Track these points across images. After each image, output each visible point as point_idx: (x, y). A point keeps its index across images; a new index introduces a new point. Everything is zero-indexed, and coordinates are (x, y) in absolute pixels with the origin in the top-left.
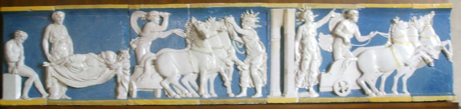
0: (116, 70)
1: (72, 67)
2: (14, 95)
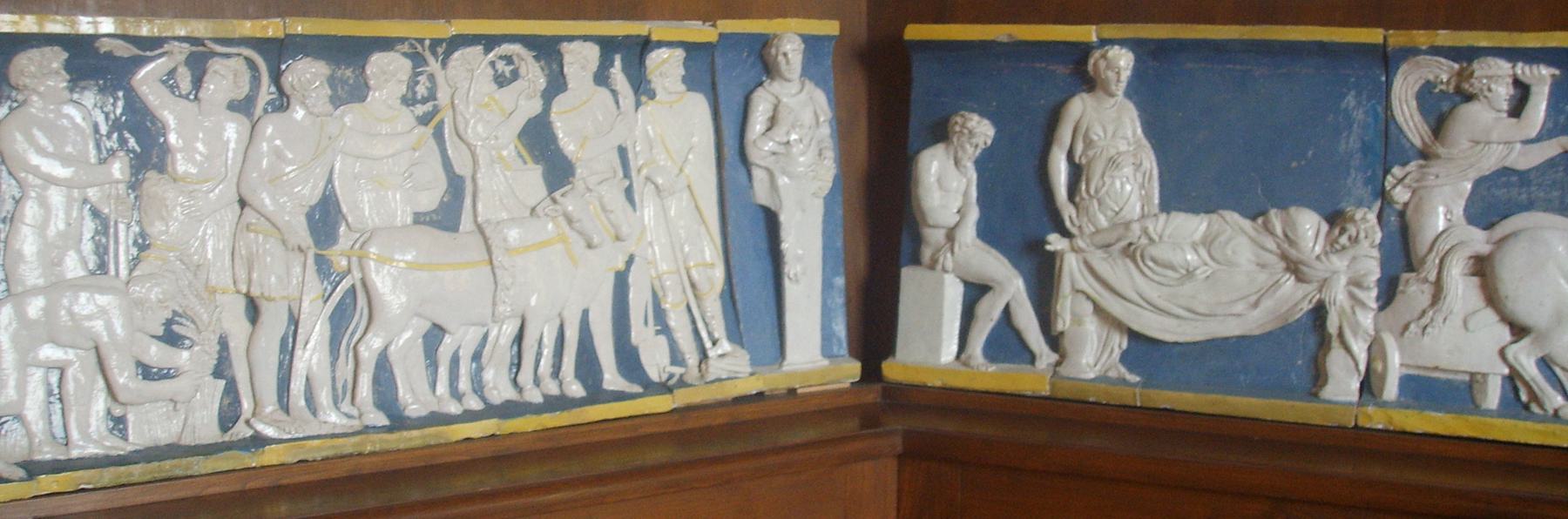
0: (1324, 284)
1: (1154, 260)
2: (936, 349)
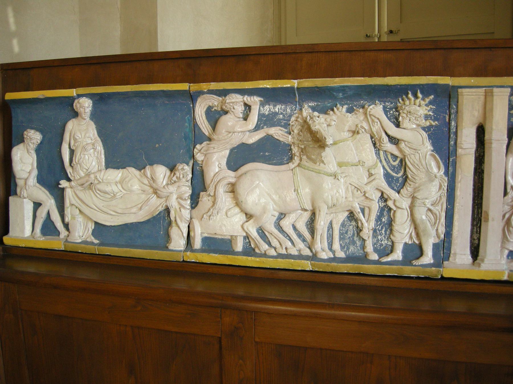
0: (167, 198)
1: (99, 190)
2: (23, 230)
